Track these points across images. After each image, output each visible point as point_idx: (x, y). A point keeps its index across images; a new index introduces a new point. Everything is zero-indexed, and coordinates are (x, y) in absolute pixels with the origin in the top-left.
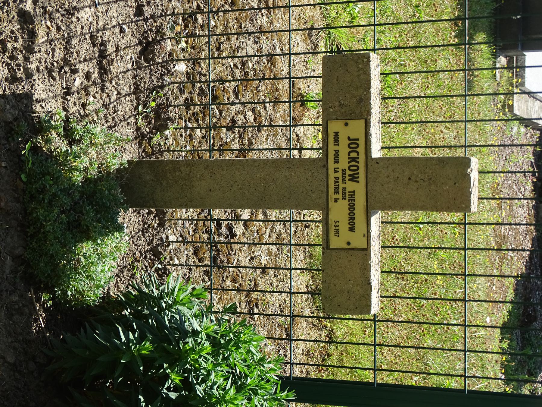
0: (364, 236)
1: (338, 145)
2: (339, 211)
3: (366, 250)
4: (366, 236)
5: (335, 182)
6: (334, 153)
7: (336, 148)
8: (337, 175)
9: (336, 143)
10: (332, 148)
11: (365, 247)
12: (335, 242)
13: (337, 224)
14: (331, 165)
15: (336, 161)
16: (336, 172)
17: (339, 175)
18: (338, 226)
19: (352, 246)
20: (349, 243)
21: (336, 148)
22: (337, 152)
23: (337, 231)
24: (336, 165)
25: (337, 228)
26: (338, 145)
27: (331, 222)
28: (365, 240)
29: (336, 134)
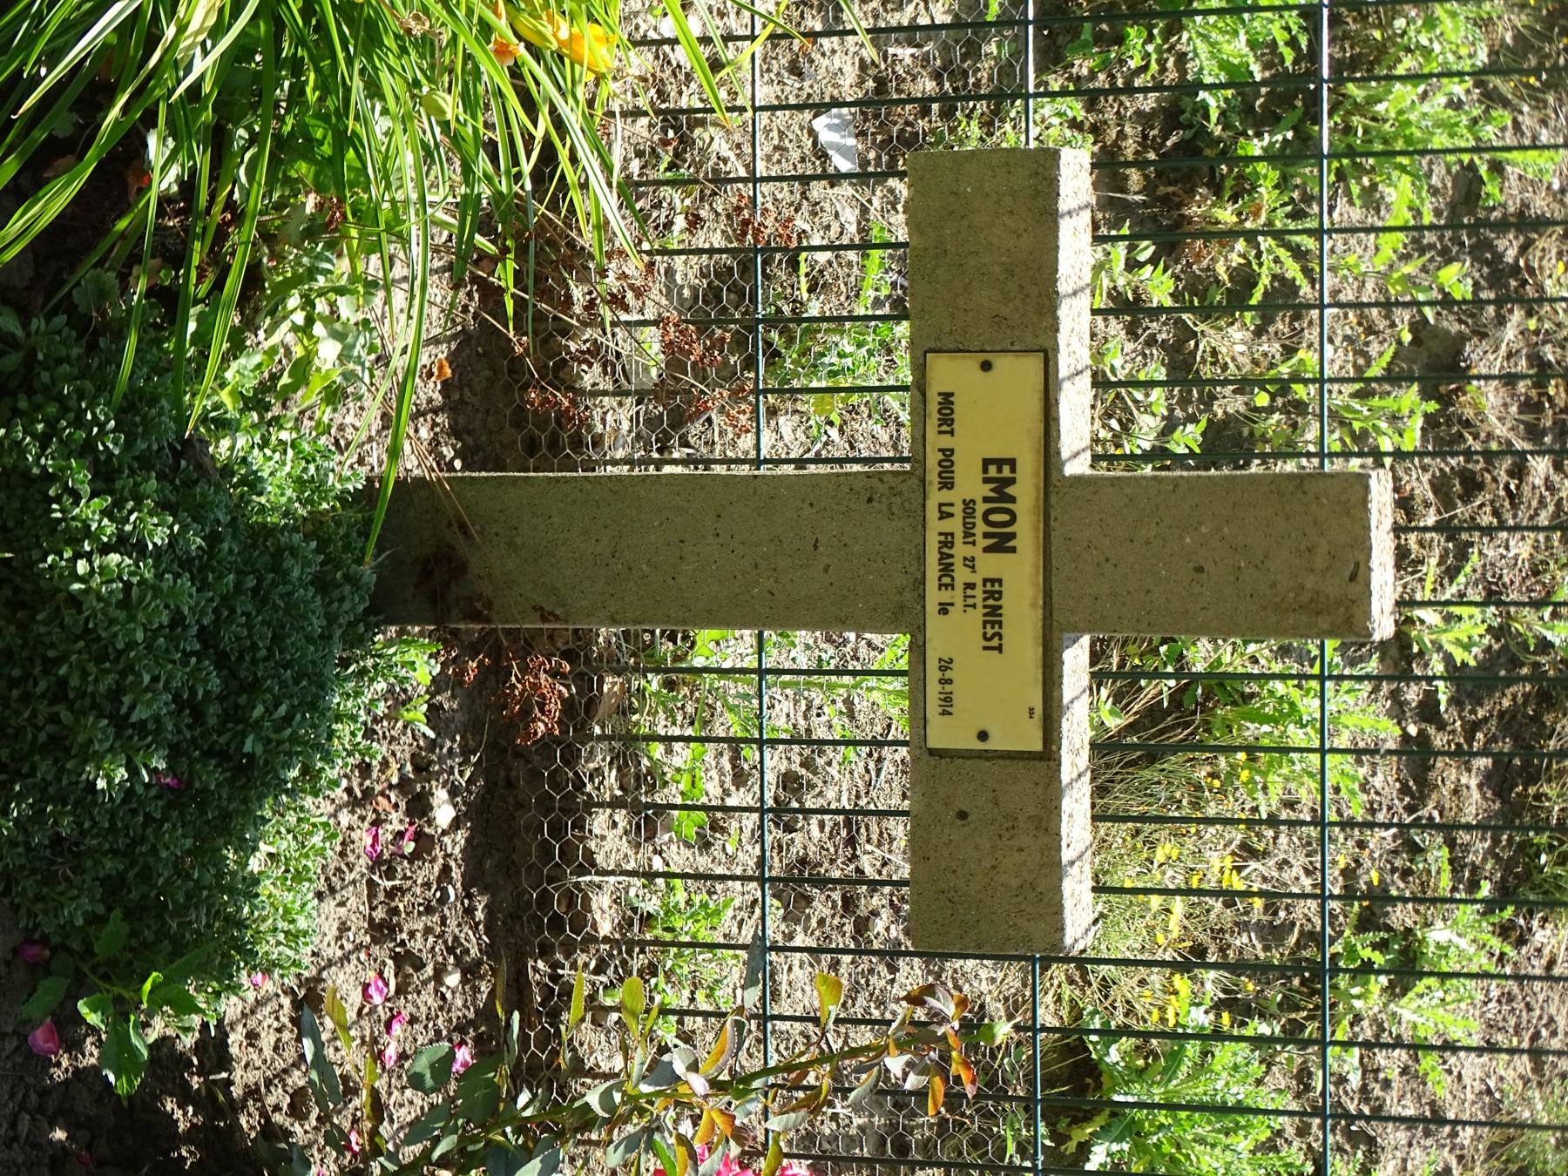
1: (952, 433)
4: (1039, 710)
5: (944, 544)
6: (940, 456)
7: (946, 442)
11: (1037, 746)
12: (942, 735)
13: (948, 674)
14: (936, 497)
15: (947, 484)
16: (944, 515)
17: (955, 525)
18: (949, 681)
20: (983, 736)
21: (946, 442)
22: (948, 453)
23: (947, 700)
24: (945, 496)
25: (948, 688)
26: (952, 433)
27: (933, 674)
29: (947, 399)
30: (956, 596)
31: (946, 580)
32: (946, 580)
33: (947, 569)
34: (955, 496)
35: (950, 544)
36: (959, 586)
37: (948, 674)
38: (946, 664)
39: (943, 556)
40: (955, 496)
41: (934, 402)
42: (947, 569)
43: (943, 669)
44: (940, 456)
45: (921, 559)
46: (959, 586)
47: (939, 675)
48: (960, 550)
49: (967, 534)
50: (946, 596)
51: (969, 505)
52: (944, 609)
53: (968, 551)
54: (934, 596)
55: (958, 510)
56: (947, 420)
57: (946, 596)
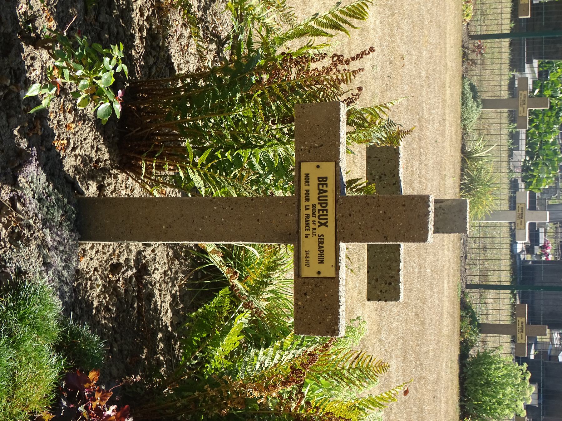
0: (332, 266)
1: (309, 185)
2: (309, 244)
3: (335, 281)
6: (305, 192)
7: (307, 188)
10: (304, 187)
12: (307, 272)
13: (308, 255)
14: (303, 203)
15: (307, 200)
17: (310, 212)
18: (308, 257)
19: (321, 275)
20: (319, 273)
21: (307, 188)
22: (308, 191)
23: (308, 262)
24: (307, 203)
25: (308, 259)
26: (309, 185)
27: (303, 254)
28: (334, 269)
29: (307, 175)
30: (310, 232)
31: (307, 228)
32: (307, 228)
33: (307, 225)
34: (310, 203)
36: (311, 229)
37: (308, 255)
38: (307, 253)
39: (306, 221)
40: (310, 203)
42: (307, 225)
43: (307, 254)
44: (305, 192)
45: (298, 221)
46: (311, 229)
47: (305, 256)
48: (311, 219)
49: (314, 214)
50: (307, 232)
51: (314, 206)
52: (307, 236)
53: (314, 219)
54: (303, 232)
55: (311, 208)
56: (307, 182)
57: (307, 232)
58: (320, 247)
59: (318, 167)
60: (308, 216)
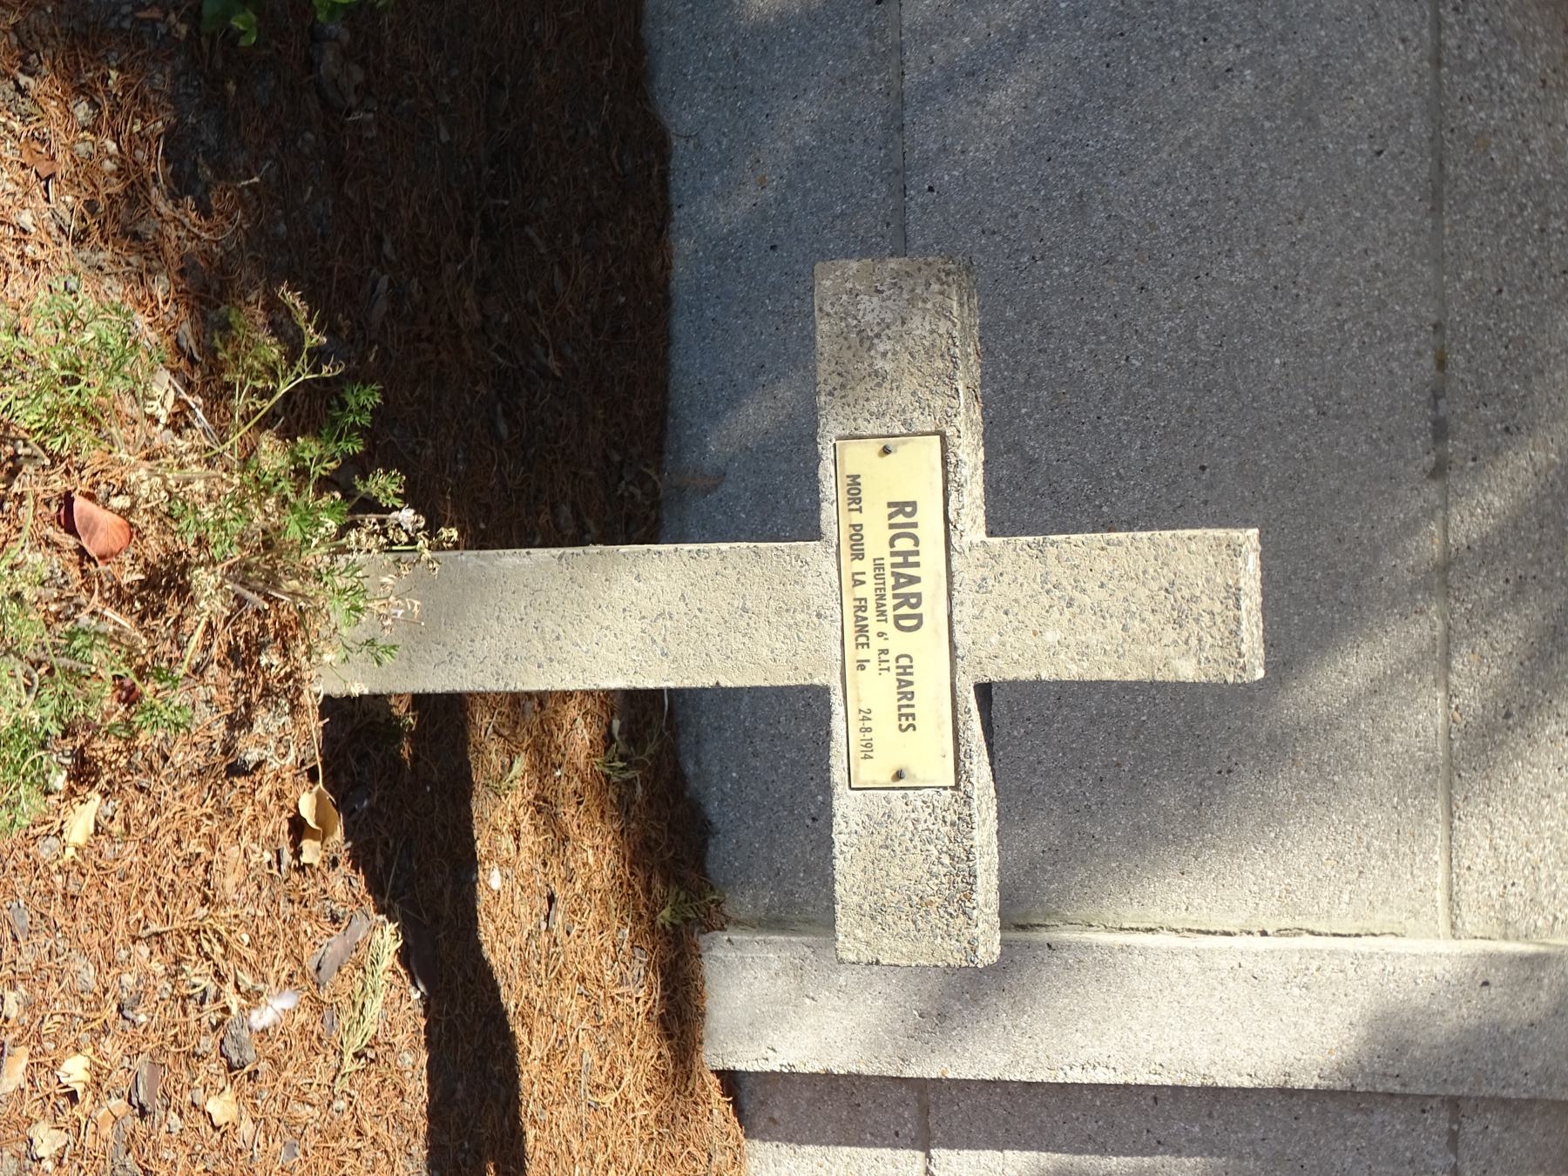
1: (860, 510)
5: (859, 608)
7: (856, 518)
8: (860, 592)
9: (854, 506)
13: (867, 724)
14: (850, 566)
15: (858, 555)
17: (868, 591)
18: (869, 730)
21: (856, 518)
22: (857, 528)
23: (868, 745)
24: (858, 566)
25: (868, 735)
26: (860, 510)
29: (855, 478)
30: (871, 654)
31: (862, 640)
32: (862, 640)
33: (862, 630)
34: (866, 565)
35: (863, 608)
37: (867, 724)
38: (866, 715)
40: (866, 565)
41: (843, 483)
42: (862, 630)
50: (863, 654)
52: (861, 666)
56: (855, 499)
58: (904, 695)
59: (886, 451)
60: (861, 606)
